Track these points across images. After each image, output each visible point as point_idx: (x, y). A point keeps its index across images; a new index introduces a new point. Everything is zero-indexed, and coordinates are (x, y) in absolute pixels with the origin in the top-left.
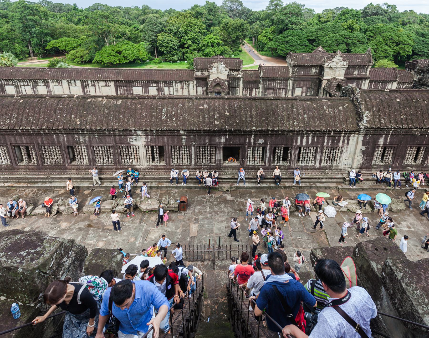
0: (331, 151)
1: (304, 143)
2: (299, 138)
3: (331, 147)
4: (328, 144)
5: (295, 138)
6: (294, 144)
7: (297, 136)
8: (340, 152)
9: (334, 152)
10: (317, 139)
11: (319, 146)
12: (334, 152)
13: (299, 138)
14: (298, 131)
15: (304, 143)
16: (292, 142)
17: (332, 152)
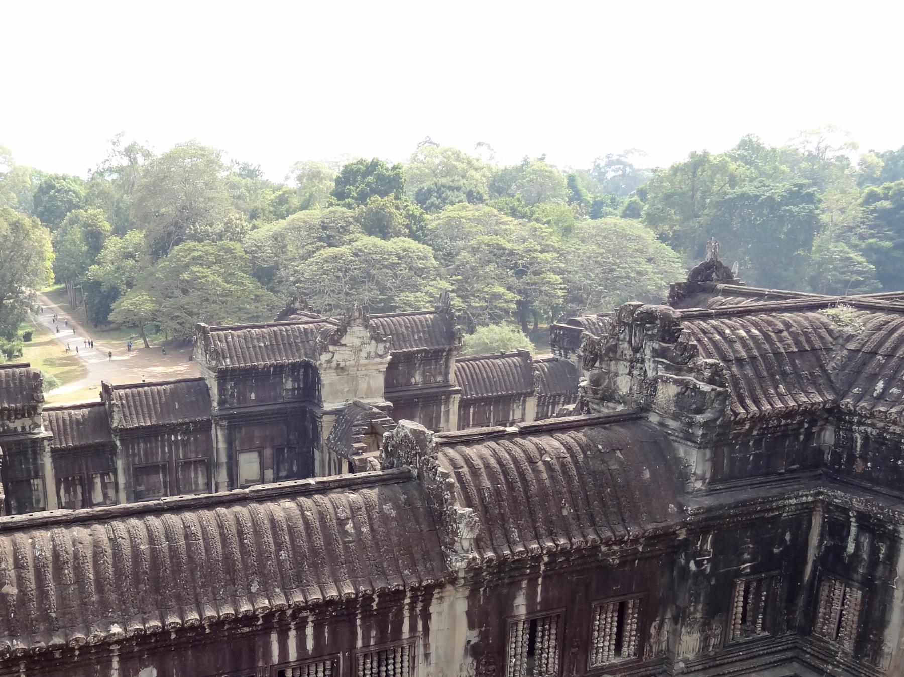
0: (379, 667)
1: (293, 655)
2: (274, 637)
3: (379, 654)
4: (366, 645)
5: (259, 641)
6: (260, 664)
7: (267, 629)
8: (406, 664)
9: (391, 667)
10: (333, 633)
11: (341, 655)
12: (391, 667)
13: (274, 637)
14: (269, 615)
15: (293, 655)
16: (253, 660)
17: (384, 669)
